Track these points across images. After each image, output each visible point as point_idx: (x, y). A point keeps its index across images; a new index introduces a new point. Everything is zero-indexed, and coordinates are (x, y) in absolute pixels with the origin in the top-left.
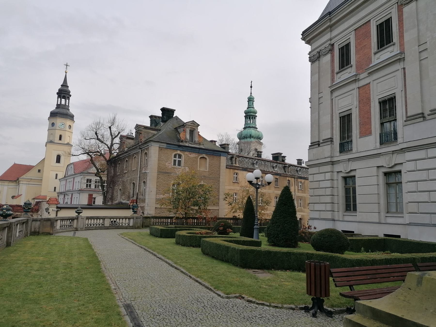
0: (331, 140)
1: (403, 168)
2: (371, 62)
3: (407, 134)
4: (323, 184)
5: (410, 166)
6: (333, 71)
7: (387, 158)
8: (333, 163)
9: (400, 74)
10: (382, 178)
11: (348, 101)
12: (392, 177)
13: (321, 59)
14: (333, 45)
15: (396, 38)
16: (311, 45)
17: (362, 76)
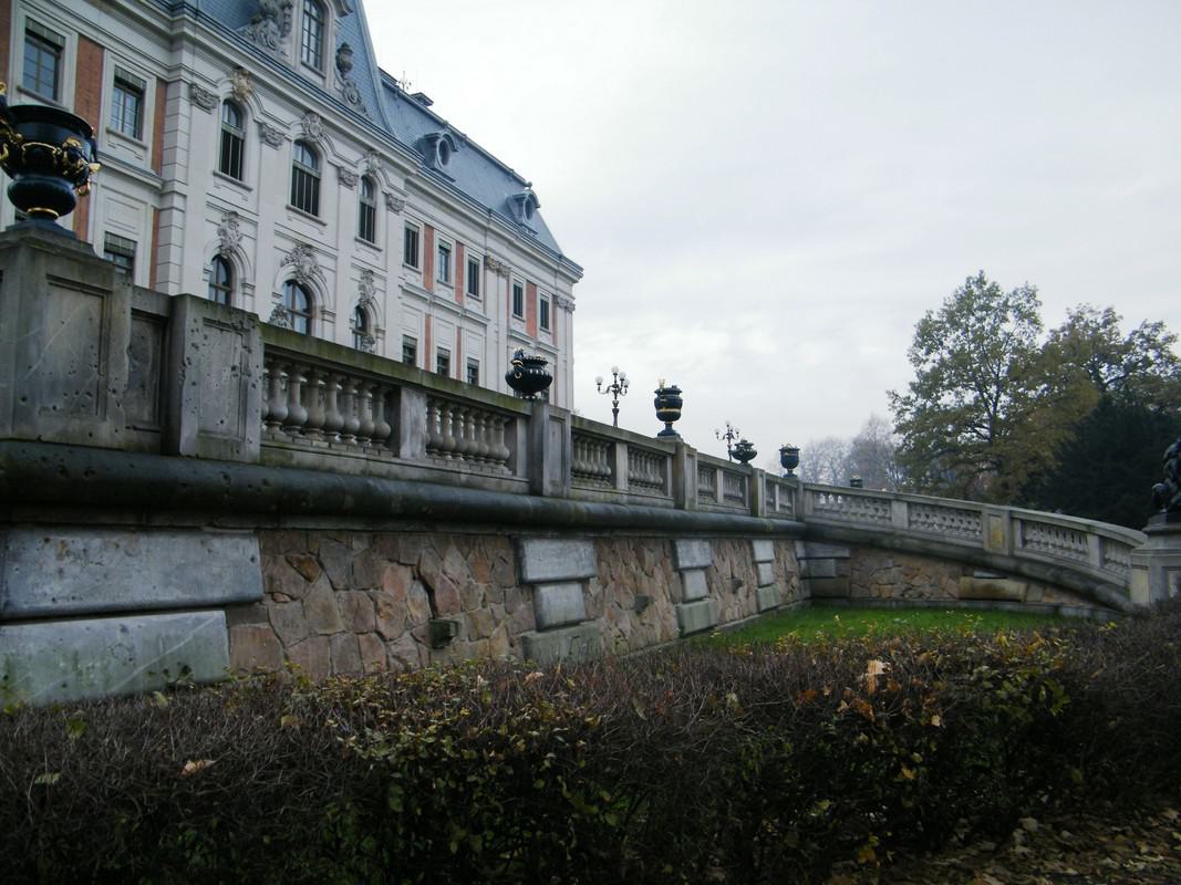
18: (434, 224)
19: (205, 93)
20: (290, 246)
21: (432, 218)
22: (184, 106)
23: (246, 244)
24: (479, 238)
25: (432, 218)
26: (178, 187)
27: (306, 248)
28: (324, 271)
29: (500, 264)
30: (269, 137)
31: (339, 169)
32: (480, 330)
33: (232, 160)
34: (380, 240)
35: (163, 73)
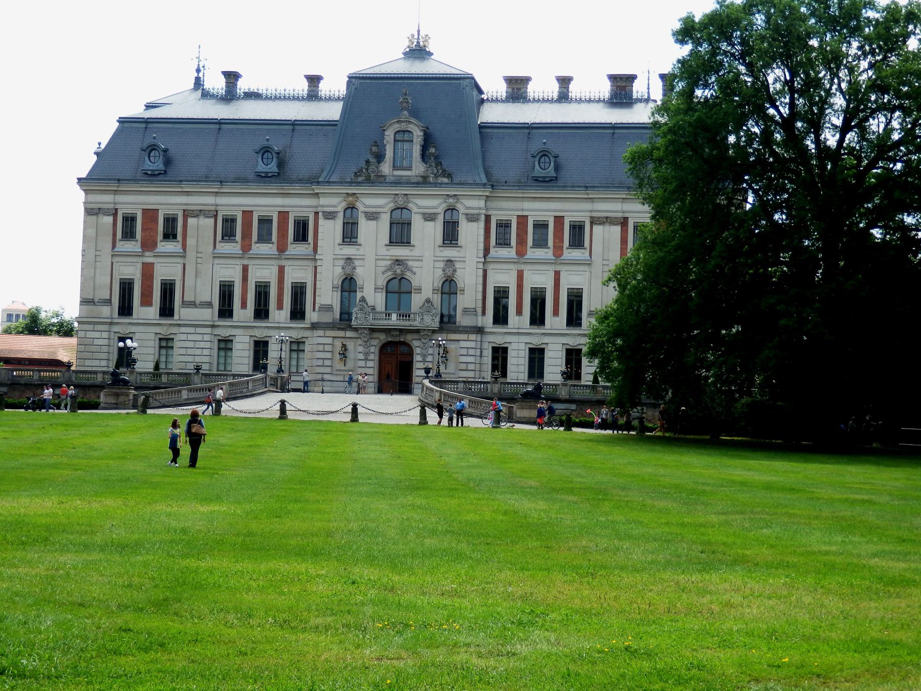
0: (108, 302)
1: (176, 338)
2: (154, 245)
3: (181, 313)
4: (97, 342)
5: (184, 337)
6: (114, 235)
7: (165, 328)
8: (111, 324)
9: (180, 267)
10: (157, 342)
11: (132, 271)
12: (166, 343)
13: (101, 216)
14: (116, 210)
15: (179, 237)
16: (86, 194)
17: (147, 254)
18: (525, 213)
19: (329, 213)
20: (389, 263)
21: (523, 210)
22: (321, 221)
23: (359, 271)
24: (587, 206)
25: (523, 210)
26: (317, 257)
27: (398, 262)
28: (414, 270)
29: (607, 218)
30: (372, 216)
31: (424, 214)
32: (586, 268)
33: (350, 235)
34: (462, 239)
35: (315, 210)
